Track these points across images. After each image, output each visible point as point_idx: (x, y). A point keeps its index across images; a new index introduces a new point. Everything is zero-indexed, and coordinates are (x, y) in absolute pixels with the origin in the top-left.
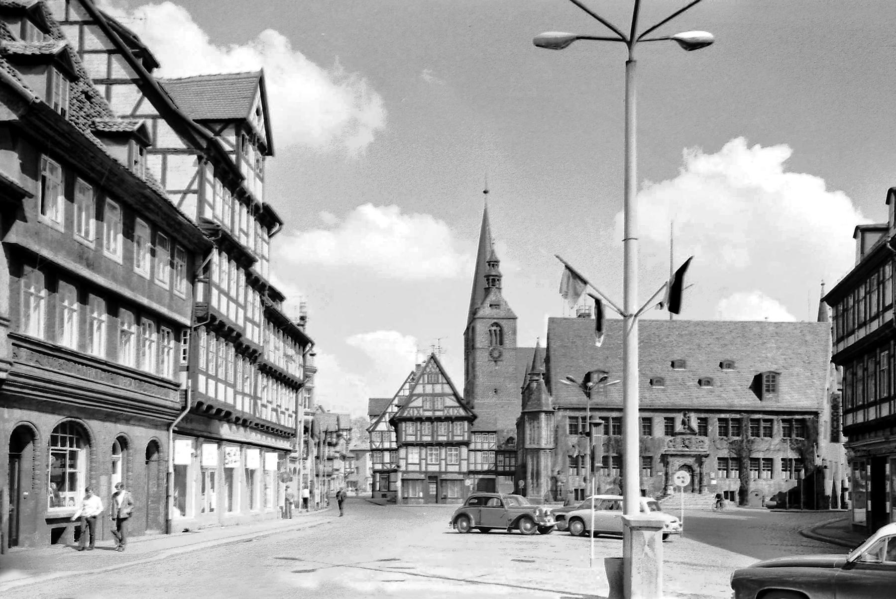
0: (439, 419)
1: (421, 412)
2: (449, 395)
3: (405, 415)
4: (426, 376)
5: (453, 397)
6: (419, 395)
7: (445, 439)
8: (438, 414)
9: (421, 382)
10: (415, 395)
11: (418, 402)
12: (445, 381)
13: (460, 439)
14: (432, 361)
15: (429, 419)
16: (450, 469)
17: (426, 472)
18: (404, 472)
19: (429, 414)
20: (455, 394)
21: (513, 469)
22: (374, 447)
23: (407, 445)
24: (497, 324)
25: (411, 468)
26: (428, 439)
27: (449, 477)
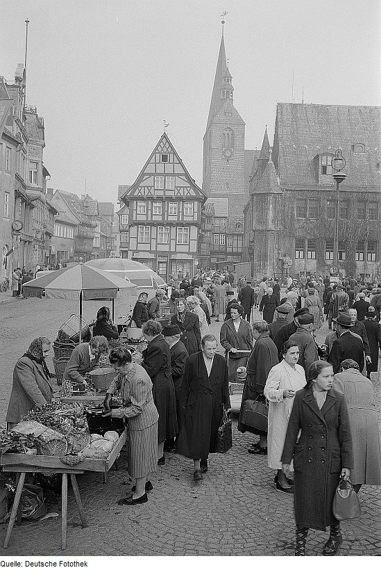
0: (170, 199)
1: (152, 191)
2: (181, 175)
5: (184, 178)
6: (150, 175)
7: (175, 219)
8: (168, 193)
10: (147, 174)
11: (148, 182)
12: (176, 161)
13: (190, 219)
14: (164, 141)
15: (160, 199)
16: (179, 249)
17: (155, 252)
18: (134, 251)
19: (161, 193)
20: (187, 174)
21: (240, 250)
22: (121, 228)
23: (137, 224)
24: (230, 129)
25: (141, 247)
26: (159, 219)
27: (178, 257)
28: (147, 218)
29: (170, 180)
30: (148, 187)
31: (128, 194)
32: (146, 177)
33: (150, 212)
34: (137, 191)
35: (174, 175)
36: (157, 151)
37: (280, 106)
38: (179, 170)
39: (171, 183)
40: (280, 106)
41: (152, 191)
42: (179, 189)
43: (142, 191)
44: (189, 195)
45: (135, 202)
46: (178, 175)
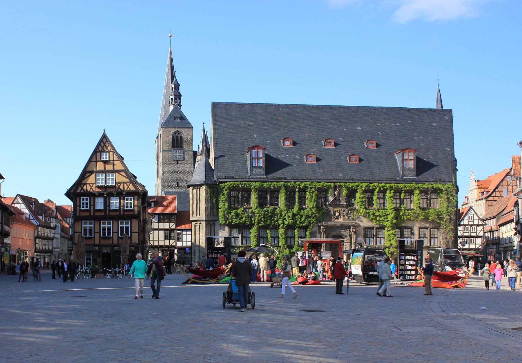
2: (122, 171)
3: (78, 191)
4: (98, 154)
5: (123, 173)
9: (94, 159)
12: (116, 158)
20: (126, 171)
28: (90, 213)
29: (110, 176)
30: (89, 184)
31: (72, 191)
32: (88, 174)
33: (92, 207)
34: (80, 188)
35: (113, 171)
36: (98, 150)
37: (215, 105)
38: (118, 166)
39: (112, 180)
40: (215, 105)
41: (94, 188)
42: (119, 185)
43: (85, 187)
44: (128, 189)
45: (78, 199)
46: (118, 171)
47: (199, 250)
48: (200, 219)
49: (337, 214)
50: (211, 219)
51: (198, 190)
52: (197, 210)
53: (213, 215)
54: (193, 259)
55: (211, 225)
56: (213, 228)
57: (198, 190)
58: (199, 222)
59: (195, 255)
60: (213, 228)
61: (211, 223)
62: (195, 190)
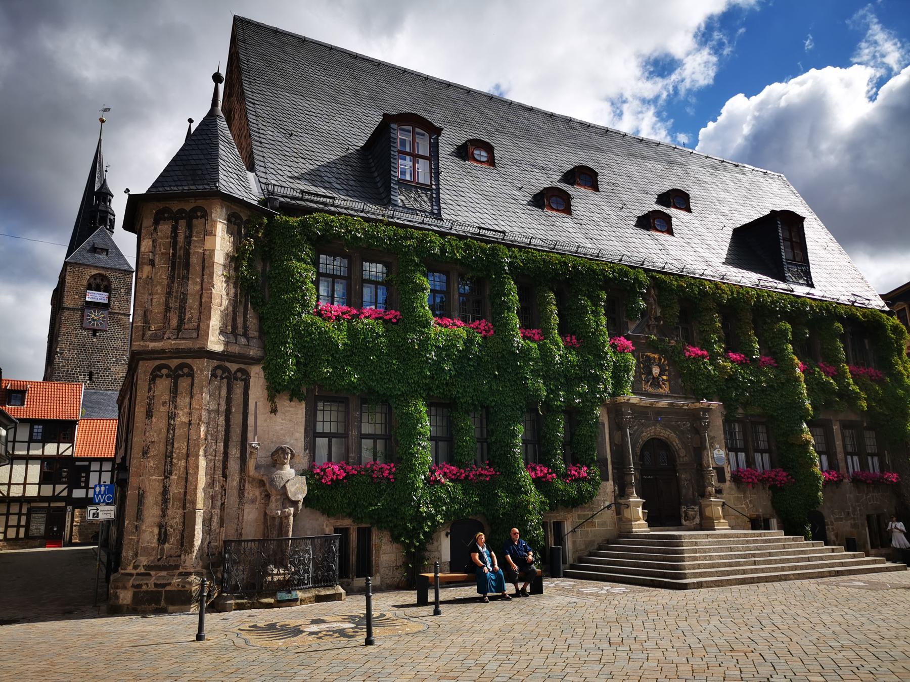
47: (165, 492)
48: (184, 344)
49: (656, 371)
50: (235, 349)
51: (182, 223)
52: (167, 309)
53: (245, 335)
54: (129, 537)
55: (231, 379)
56: (238, 390)
57: (182, 223)
58: (174, 363)
59: (139, 516)
60: (238, 390)
61: (233, 367)
62: (165, 228)
